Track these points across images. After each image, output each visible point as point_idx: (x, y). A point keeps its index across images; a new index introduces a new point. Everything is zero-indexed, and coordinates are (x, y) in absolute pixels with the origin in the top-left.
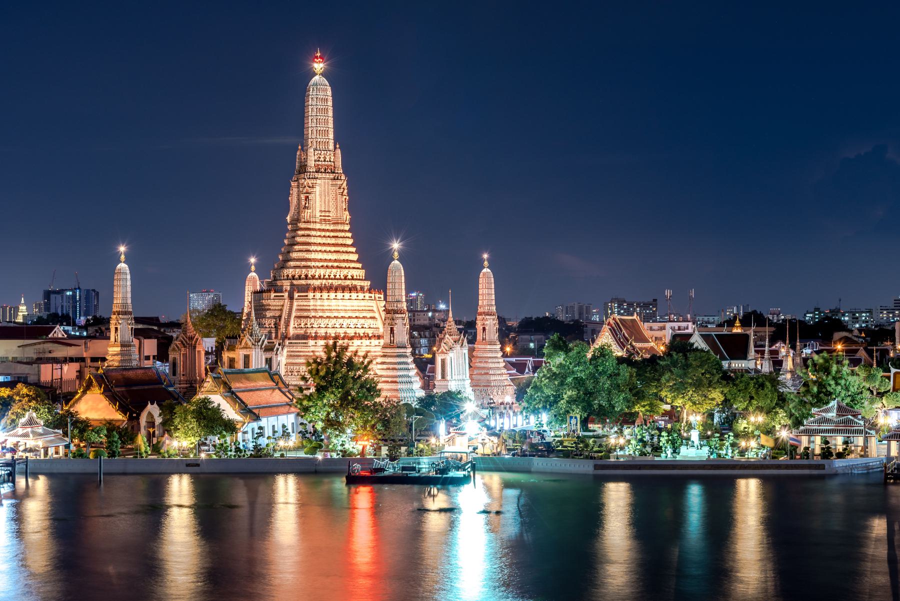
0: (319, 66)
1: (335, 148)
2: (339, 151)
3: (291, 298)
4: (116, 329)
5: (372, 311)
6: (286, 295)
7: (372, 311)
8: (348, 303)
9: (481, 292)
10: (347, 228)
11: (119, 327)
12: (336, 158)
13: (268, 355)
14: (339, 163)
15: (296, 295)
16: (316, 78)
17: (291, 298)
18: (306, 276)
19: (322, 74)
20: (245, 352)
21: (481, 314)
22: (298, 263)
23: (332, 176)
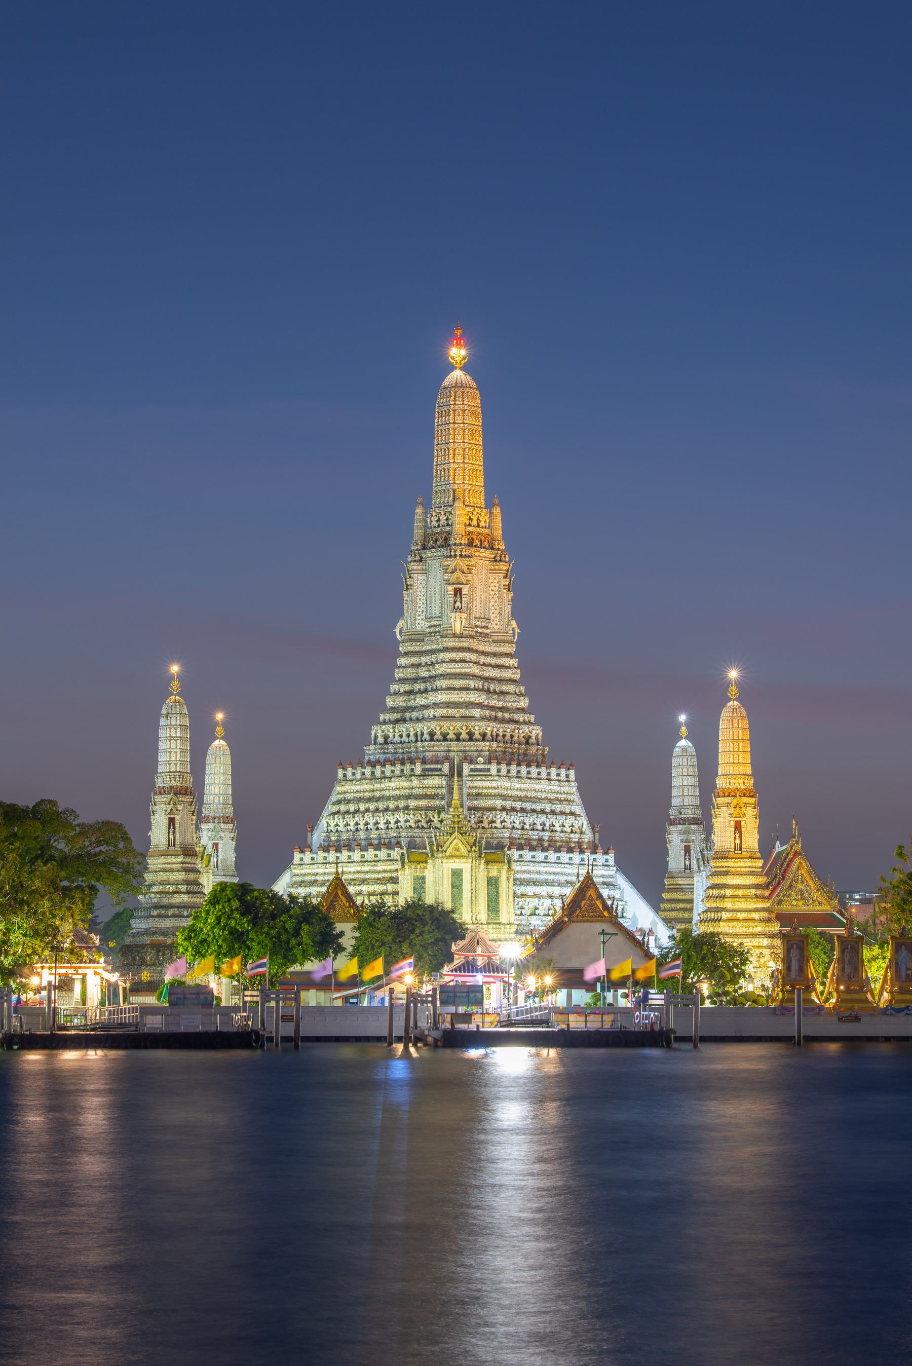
0: (457, 353)
1: (489, 505)
2: (497, 511)
4: (172, 821)
5: (570, 802)
7: (570, 802)
8: (544, 786)
9: (675, 782)
11: (178, 817)
12: (494, 522)
14: (498, 532)
16: (457, 375)
18: (471, 735)
19: (464, 368)
20: (456, 864)
21: (672, 823)
22: (452, 712)
23: (491, 554)
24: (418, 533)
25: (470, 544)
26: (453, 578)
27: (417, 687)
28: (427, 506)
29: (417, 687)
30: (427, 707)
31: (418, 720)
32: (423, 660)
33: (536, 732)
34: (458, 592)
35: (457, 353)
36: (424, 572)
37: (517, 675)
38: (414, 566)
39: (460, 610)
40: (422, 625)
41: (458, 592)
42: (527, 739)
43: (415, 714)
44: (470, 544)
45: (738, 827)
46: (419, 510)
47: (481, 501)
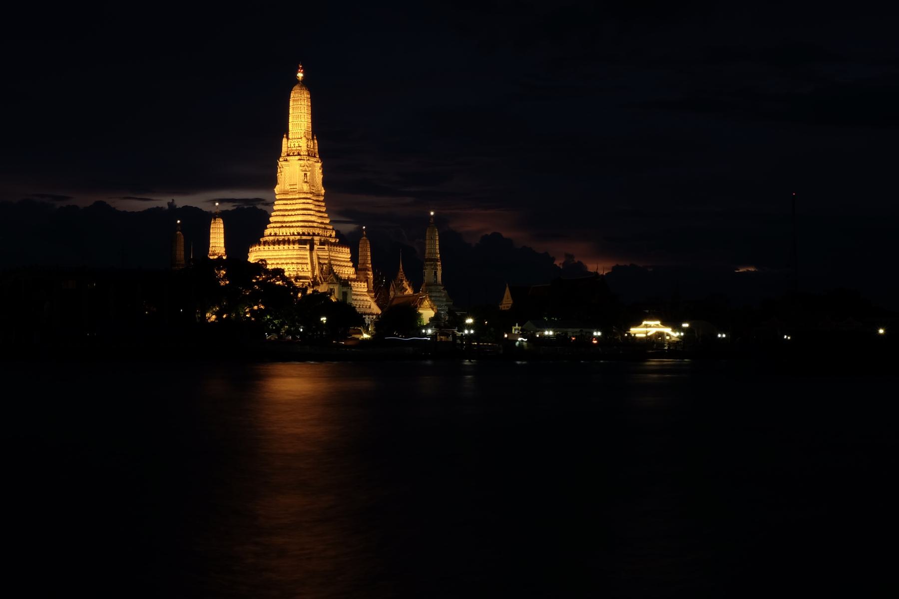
1: (313, 139)
3: (312, 249)
6: (308, 247)
10: (322, 198)
13: (345, 289)
15: (316, 247)
17: (312, 249)
24: (284, 149)
25: (309, 155)
26: (304, 169)
27: (286, 213)
28: (288, 138)
29: (286, 213)
30: (291, 222)
31: (292, 227)
32: (288, 202)
33: (334, 234)
34: (305, 174)
35: (300, 75)
36: (288, 166)
37: (324, 209)
38: (284, 163)
39: (306, 182)
40: (288, 188)
41: (305, 174)
42: (330, 236)
43: (288, 225)
44: (309, 155)
45: (435, 273)
46: (285, 140)
47: (310, 137)
